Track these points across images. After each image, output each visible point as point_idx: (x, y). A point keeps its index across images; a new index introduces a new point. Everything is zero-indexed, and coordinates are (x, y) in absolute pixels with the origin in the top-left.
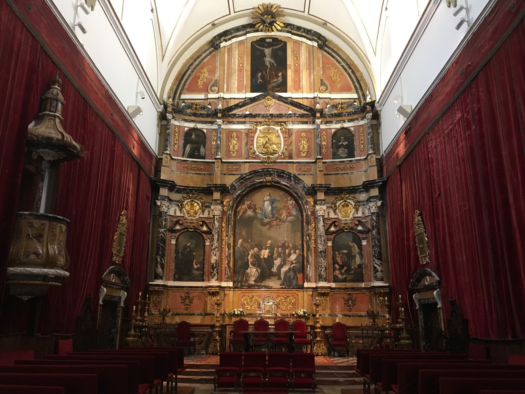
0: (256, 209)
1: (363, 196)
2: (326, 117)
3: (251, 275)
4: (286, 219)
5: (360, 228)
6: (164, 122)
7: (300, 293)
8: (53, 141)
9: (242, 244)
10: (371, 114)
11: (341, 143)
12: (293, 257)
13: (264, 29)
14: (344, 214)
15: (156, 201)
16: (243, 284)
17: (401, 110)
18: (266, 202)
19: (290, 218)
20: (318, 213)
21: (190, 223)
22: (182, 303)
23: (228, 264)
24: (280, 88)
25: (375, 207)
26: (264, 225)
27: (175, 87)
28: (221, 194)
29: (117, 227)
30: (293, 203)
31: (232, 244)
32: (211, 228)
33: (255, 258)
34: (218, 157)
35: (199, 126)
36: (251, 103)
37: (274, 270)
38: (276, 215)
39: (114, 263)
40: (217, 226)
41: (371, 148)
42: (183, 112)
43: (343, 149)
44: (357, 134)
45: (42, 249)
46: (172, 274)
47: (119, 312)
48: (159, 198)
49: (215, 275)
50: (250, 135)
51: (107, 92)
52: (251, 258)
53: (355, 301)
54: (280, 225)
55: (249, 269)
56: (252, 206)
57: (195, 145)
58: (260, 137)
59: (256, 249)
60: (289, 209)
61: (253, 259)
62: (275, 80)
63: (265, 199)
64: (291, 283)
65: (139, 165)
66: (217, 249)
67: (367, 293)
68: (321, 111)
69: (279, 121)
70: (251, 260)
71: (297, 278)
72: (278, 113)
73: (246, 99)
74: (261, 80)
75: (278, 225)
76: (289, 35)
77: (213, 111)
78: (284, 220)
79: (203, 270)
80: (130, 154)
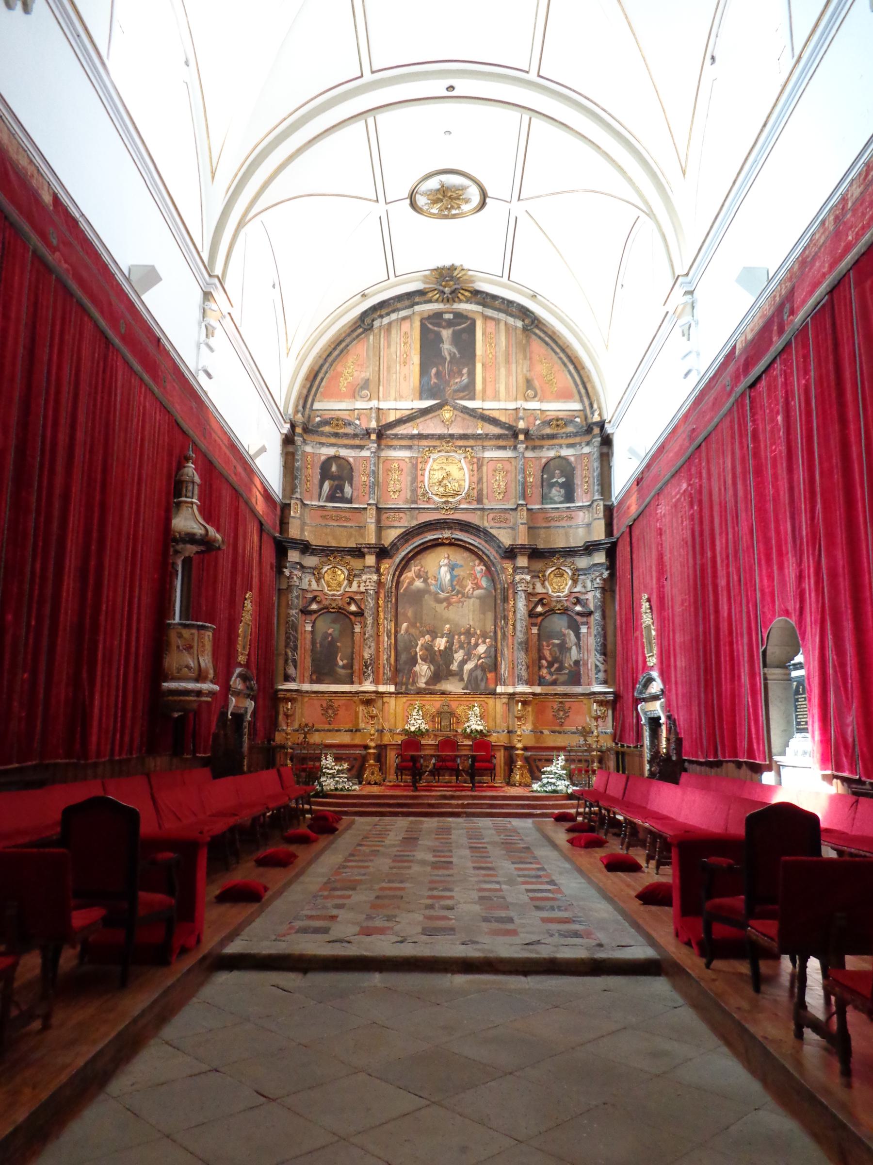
0: (428, 578)
1: (583, 562)
2: (533, 439)
3: (421, 675)
4: (472, 593)
5: (578, 608)
6: (291, 449)
7: (491, 701)
8: (196, 537)
9: (407, 631)
10: (599, 439)
11: (555, 480)
12: (482, 649)
13: (440, 299)
14: (556, 587)
15: (285, 570)
16: (409, 687)
17: (632, 451)
18: (443, 568)
19: (478, 592)
20: (519, 585)
21: (332, 599)
22: (322, 714)
23: (388, 659)
24: (464, 394)
25: (600, 579)
26: (439, 601)
27: (305, 392)
28: (377, 557)
29: (242, 617)
30: (482, 569)
31: (393, 631)
32: (363, 607)
33: (426, 649)
34: (371, 501)
35: (343, 452)
36: (419, 418)
37: (454, 667)
38: (457, 588)
39: (240, 665)
40: (371, 605)
41: (598, 491)
42: (317, 431)
43: (558, 489)
44: (579, 466)
45: (193, 661)
46: (307, 674)
47: (246, 727)
48: (288, 565)
49: (369, 675)
50: (420, 466)
51: (229, 438)
52: (421, 650)
53: (567, 713)
54: (463, 602)
55: (417, 665)
56: (422, 573)
57: (336, 483)
58: (434, 470)
59: (428, 637)
60: (476, 578)
61: (424, 651)
62: (456, 381)
63: (441, 564)
64: (477, 685)
65: (261, 524)
66: (371, 639)
67: (585, 701)
68: (526, 433)
69: (462, 445)
70: (421, 653)
71: (487, 679)
72: (461, 432)
73: (414, 411)
74: (437, 379)
75: (459, 602)
76: (479, 308)
77: (363, 429)
78: (469, 595)
79: (352, 667)
80: (253, 512)
